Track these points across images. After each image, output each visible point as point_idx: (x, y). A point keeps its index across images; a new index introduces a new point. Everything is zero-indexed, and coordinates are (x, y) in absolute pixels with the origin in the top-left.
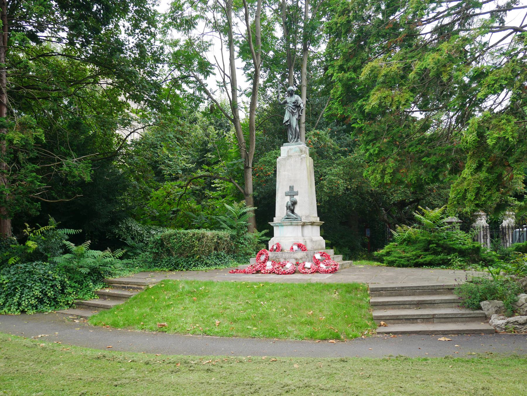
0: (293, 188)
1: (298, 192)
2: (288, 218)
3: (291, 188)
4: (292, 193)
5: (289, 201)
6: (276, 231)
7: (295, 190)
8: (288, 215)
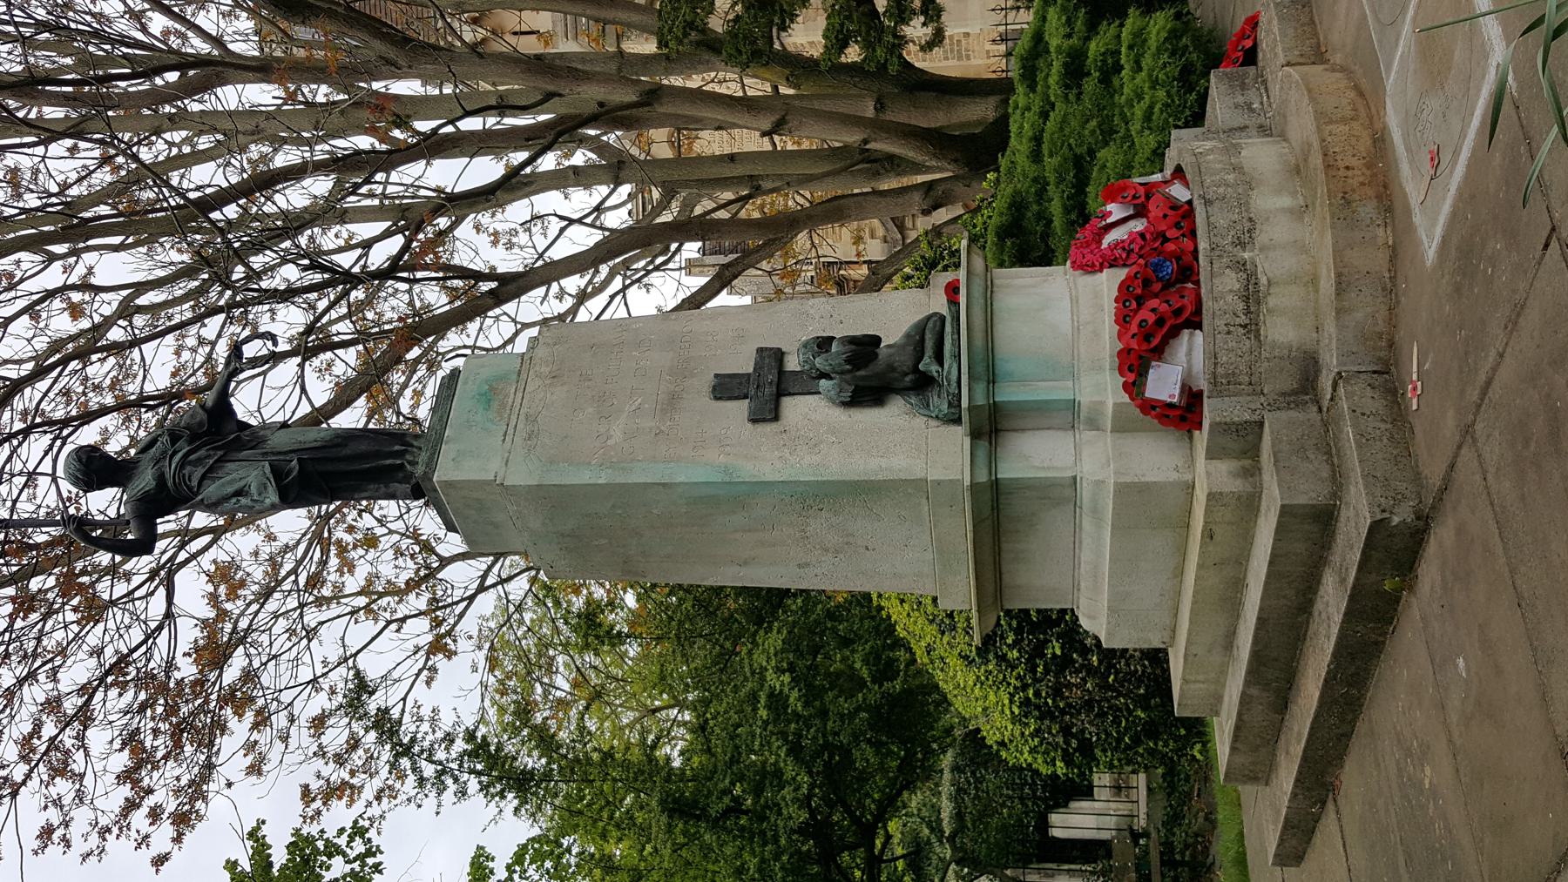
3: (726, 388)
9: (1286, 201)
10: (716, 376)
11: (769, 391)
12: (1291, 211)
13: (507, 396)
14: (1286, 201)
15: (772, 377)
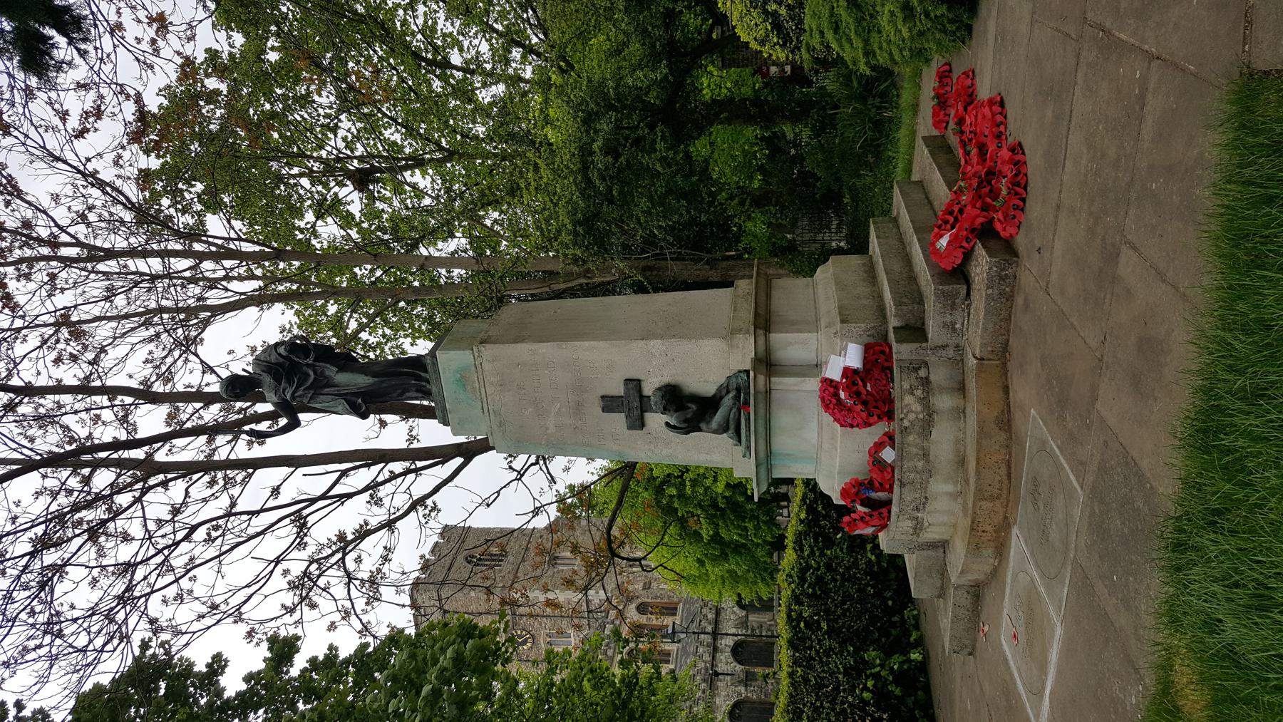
2: (733, 428)
3: (610, 404)
5: (665, 418)
7: (619, 390)
8: (724, 429)
9: (949, 488)
10: (603, 397)
11: (636, 413)
12: (950, 494)
14: (949, 488)
15: (636, 404)
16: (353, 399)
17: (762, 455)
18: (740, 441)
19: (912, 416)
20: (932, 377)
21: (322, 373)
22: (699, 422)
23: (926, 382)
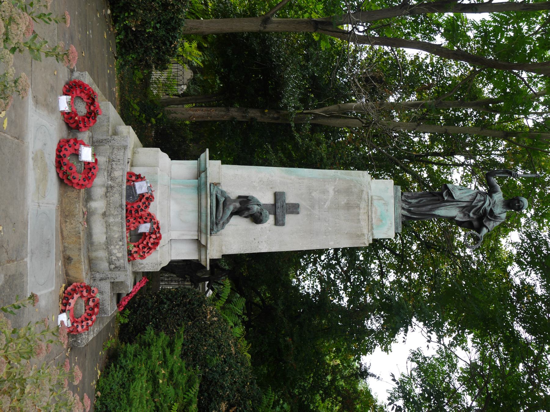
0: (292, 213)
1: (283, 224)
3: (294, 209)
4: (281, 209)
6: (185, 167)
7: (289, 218)
10: (298, 213)
11: (279, 205)
13: (375, 217)
15: (278, 211)
16: (450, 199)
17: (203, 193)
18: (216, 196)
19: (117, 247)
20: (107, 264)
21: (465, 215)
22: (240, 208)
23: (110, 263)
